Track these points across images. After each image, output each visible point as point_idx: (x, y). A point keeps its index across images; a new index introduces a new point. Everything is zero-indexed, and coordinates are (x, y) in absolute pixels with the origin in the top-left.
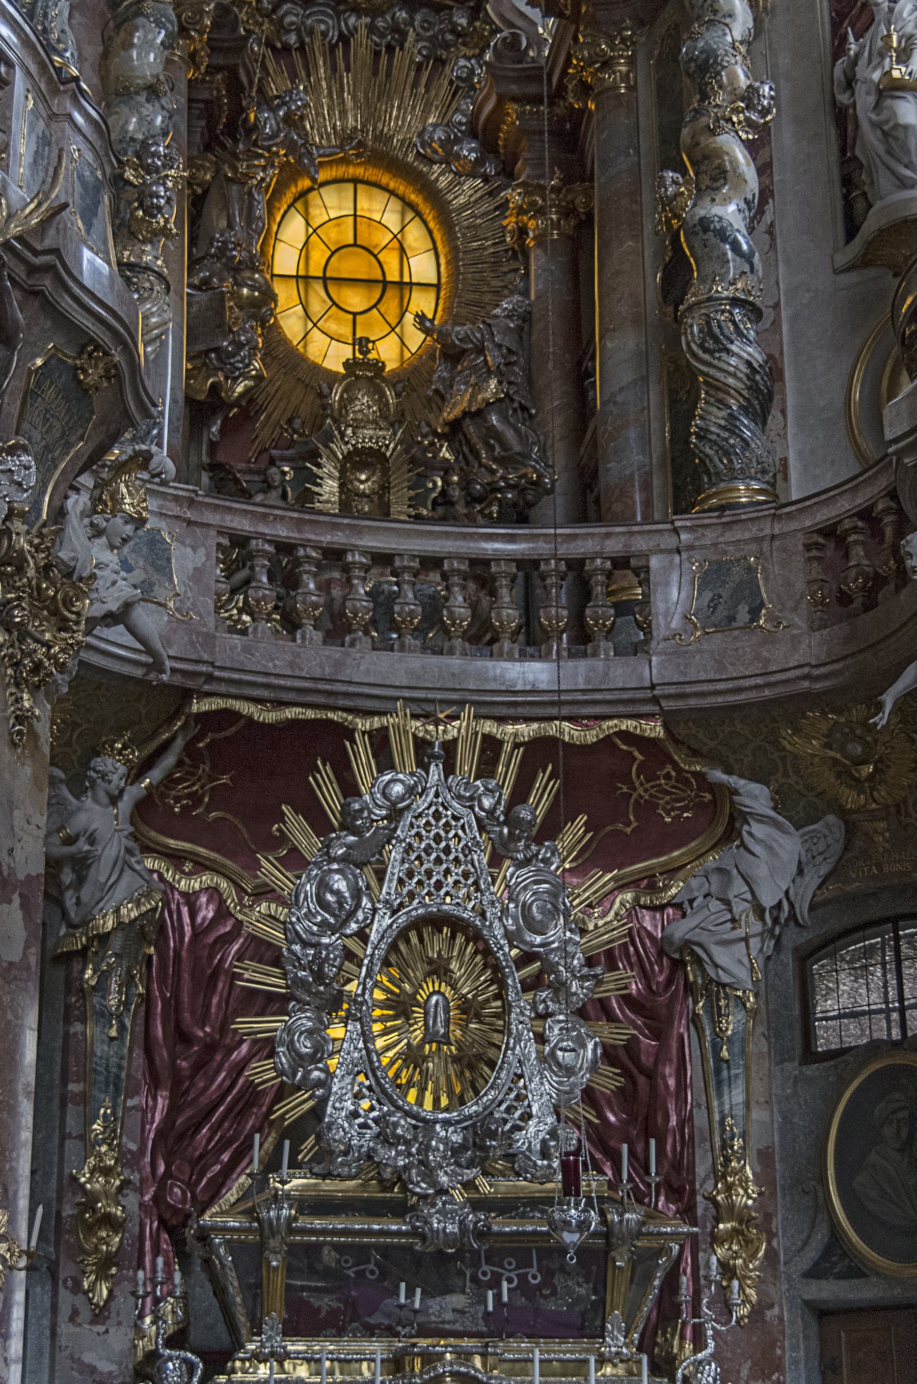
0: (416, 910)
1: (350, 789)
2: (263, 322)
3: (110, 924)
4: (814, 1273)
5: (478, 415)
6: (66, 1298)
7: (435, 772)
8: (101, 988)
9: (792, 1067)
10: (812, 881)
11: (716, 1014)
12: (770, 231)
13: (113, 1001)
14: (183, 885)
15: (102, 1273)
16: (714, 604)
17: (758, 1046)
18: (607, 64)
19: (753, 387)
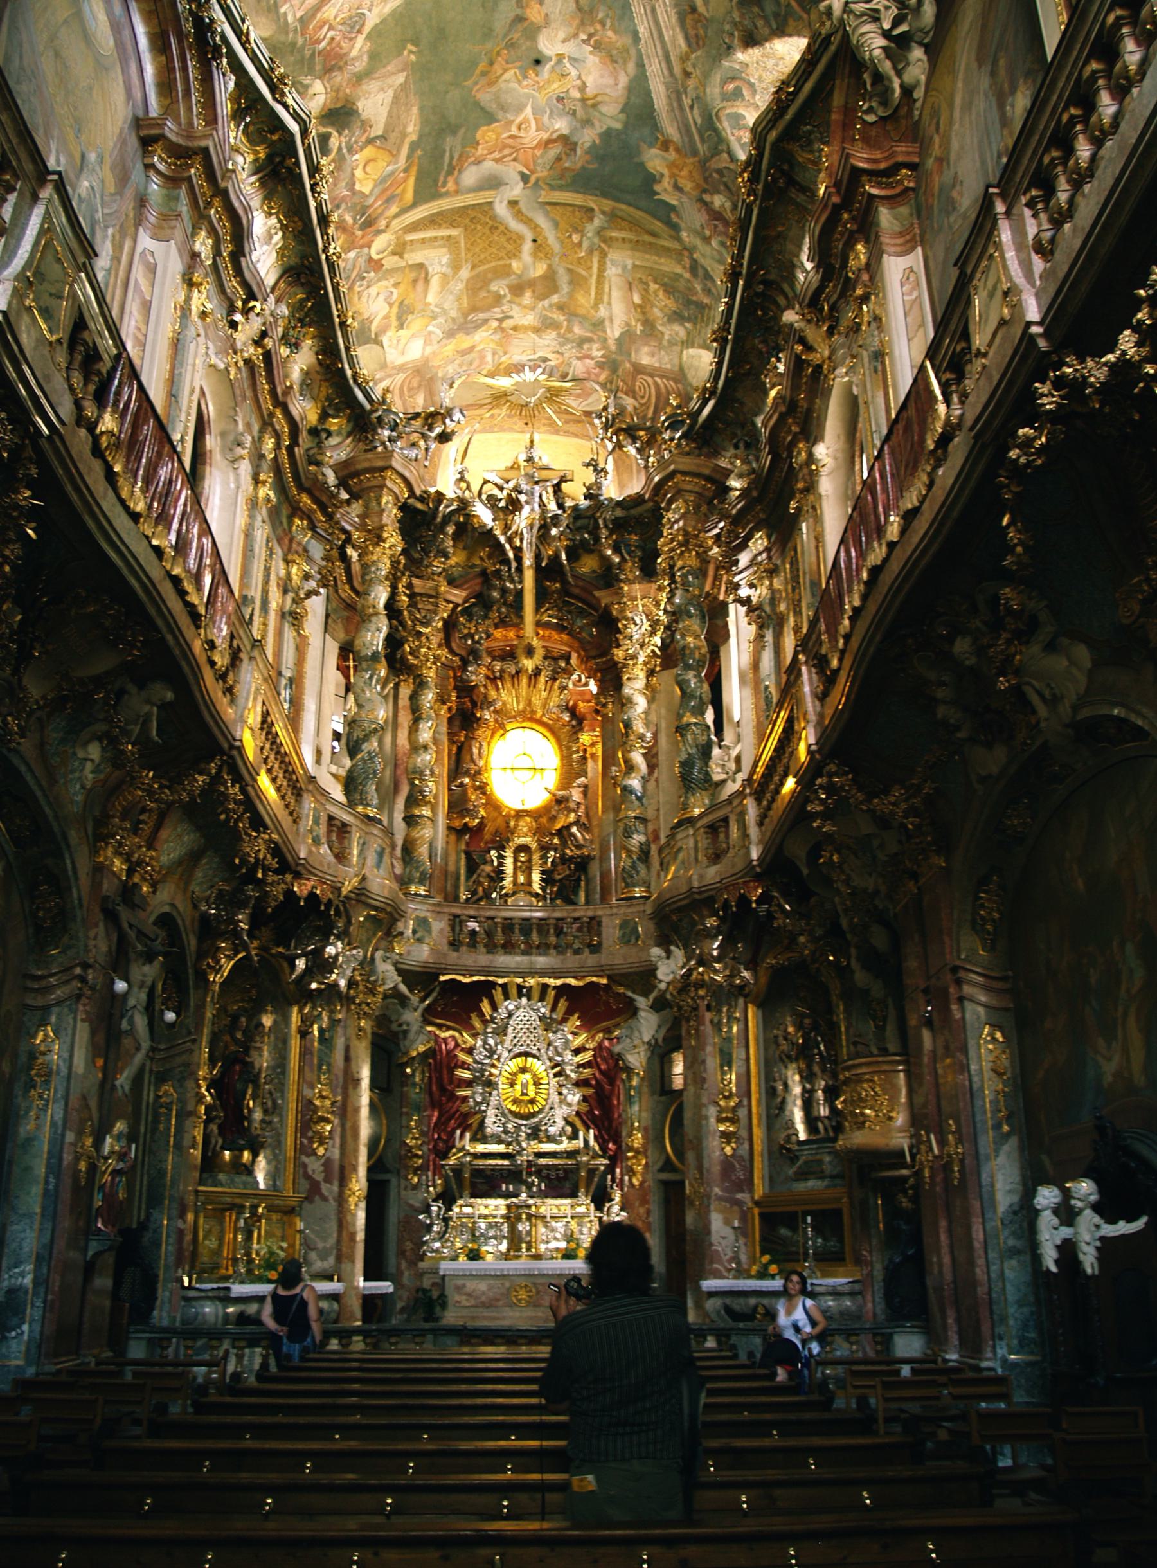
0: (516, 1050)
1: (495, 1008)
2: (484, 793)
3: (414, 1054)
4: (661, 1170)
5: (568, 827)
6: (403, 1182)
7: (524, 1000)
8: (413, 1075)
9: (656, 1097)
10: (663, 1032)
11: (630, 1079)
12: (657, 780)
13: (417, 1079)
14: (443, 1035)
15: (415, 1174)
16: (624, 935)
17: (645, 1090)
18: (604, 705)
19: (641, 850)
